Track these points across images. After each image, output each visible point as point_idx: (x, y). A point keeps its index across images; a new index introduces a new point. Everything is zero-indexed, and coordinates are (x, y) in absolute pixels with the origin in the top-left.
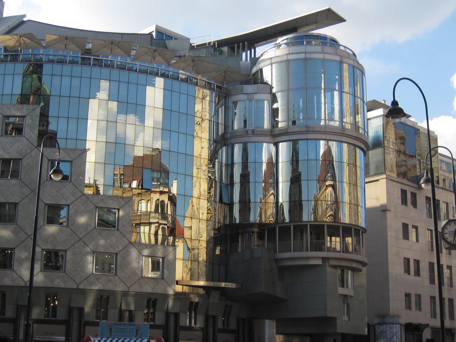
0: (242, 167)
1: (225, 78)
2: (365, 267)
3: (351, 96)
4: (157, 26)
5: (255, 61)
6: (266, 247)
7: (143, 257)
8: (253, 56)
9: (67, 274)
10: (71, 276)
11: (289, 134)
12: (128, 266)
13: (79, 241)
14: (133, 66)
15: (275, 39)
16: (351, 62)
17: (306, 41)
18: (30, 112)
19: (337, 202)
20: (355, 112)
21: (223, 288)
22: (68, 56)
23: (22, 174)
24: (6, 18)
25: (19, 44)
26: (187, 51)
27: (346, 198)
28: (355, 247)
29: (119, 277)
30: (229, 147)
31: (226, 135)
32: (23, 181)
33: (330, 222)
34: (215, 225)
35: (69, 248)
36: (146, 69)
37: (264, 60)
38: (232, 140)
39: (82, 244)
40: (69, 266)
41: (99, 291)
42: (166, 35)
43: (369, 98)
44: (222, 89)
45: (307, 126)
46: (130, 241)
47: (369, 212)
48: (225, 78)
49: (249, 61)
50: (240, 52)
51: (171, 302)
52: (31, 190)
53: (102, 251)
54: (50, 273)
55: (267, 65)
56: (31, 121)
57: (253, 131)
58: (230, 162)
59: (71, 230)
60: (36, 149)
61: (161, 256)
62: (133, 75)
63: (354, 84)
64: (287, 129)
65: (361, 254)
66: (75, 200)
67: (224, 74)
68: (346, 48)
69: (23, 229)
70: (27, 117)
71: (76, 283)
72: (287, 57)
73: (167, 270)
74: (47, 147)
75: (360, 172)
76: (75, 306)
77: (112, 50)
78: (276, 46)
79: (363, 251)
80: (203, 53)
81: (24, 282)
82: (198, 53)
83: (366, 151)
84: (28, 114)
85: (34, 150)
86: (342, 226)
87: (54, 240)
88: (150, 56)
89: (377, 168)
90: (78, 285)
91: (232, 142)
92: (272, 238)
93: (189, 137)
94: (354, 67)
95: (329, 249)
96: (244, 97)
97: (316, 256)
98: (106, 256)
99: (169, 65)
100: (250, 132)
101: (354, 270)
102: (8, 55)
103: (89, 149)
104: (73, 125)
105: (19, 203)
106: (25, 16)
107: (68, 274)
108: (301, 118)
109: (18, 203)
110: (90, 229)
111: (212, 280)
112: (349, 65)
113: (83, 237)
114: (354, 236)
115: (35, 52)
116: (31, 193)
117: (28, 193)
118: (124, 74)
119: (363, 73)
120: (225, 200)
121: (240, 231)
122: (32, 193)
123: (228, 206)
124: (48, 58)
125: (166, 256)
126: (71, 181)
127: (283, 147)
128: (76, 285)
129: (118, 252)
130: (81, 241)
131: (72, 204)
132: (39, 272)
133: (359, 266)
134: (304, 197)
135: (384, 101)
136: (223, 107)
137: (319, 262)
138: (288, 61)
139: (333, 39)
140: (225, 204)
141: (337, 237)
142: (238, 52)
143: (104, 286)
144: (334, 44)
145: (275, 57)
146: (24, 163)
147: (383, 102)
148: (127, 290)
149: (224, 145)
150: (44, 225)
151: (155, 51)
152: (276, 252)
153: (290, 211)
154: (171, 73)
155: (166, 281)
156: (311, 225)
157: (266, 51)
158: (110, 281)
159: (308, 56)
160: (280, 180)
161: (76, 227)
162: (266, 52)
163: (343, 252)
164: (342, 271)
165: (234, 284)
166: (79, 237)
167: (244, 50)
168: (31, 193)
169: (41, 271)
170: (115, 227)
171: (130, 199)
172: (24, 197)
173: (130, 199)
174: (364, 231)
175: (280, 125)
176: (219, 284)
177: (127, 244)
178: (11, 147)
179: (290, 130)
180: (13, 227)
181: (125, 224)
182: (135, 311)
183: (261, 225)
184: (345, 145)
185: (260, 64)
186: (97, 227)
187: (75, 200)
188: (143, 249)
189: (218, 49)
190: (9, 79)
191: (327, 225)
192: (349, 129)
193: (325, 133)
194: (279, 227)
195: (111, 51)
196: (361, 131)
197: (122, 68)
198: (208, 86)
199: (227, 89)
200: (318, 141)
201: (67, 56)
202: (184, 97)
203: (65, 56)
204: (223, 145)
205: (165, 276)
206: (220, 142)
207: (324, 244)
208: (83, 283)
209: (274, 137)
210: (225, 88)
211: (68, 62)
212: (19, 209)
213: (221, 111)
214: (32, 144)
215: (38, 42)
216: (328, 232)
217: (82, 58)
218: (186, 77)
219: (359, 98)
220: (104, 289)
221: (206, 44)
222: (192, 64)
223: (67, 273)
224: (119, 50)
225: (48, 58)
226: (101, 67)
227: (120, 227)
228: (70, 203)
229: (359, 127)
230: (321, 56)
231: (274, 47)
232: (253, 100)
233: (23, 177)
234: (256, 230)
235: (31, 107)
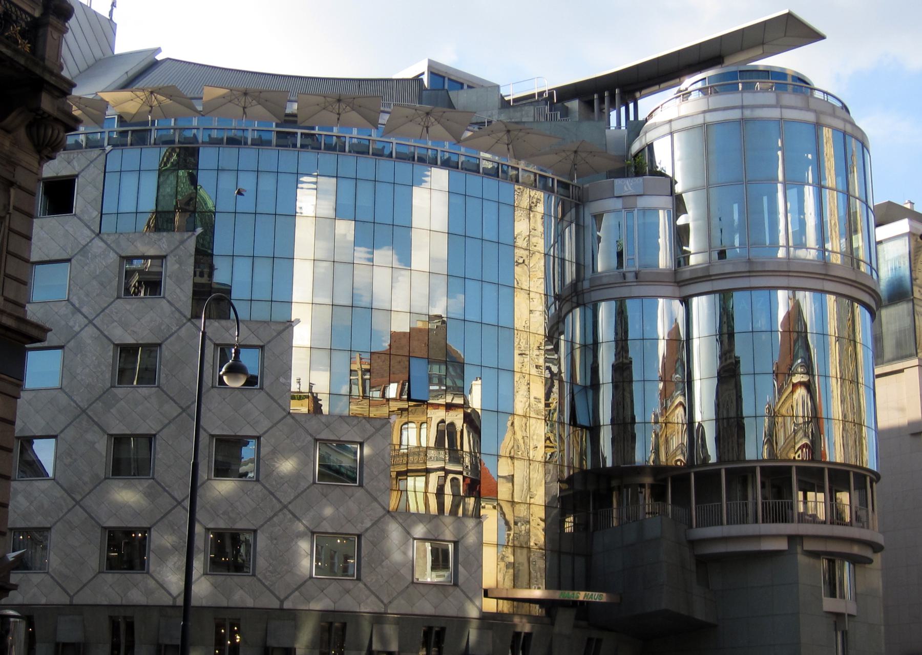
0: (616, 348)
1: (575, 165)
2: (879, 554)
3: (841, 195)
4: (430, 61)
5: (636, 127)
6: (670, 516)
7: (415, 541)
8: (632, 118)
9: (259, 580)
10: (266, 584)
11: (713, 278)
12: (383, 561)
13: (281, 510)
14: (384, 147)
15: (677, 80)
16: (839, 124)
17: (743, 83)
18: (175, 249)
19: (816, 419)
20: (850, 229)
21: (582, 602)
22: (250, 129)
23: (163, 376)
24: (121, 56)
25: (149, 108)
26: (496, 112)
27: (836, 409)
28: (856, 512)
29: (365, 585)
30: (586, 308)
31: (580, 284)
32: (165, 389)
33: (802, 460)
34: (562, 471)
35: (262, 525)
36: (411, 152)
37: (655, 126)
38: (592, 293)
39: (288, 517)
40: (261, 563)
41: (324, 613)
42: (449, 79)
43: (878, 198)
44: (569, 189)
45: (750, 261)
46: (387, 508)
47: (885, 437)
48: (575, 165)
49: (624, 128)
50: (604, 111)
51: (473, 634)
52: (181, 407)
53: (330, 531)
54: (224, 576)
55: (664, 136)
56: (177, 266)
57: (637, 275)
58: (590, 340)
60: (189, 323)
61: (452, 539)
62: (385, 165)
63: (845, 170)
64: (707, 268)
65: (871, 525)
66: (271, 428)
67: (572, 157)
68: (828, 94)
69: (167, 489)
70: (168, 258)
71: (278, 598)
72: (704, 117)
73: (464, 567)
74: (213, 319)
75: (864, 354)
76: (276, 645)
77: (339, 114)
78: (680, 96)
79: (874, 520)
80: (528, 114)
81: (170, 597)
82: (518, 114)
83: (875, 309)
84: (172, 252)
85: (184, 324)
86: (829, 469)
87: (230, 509)
88: (419, 124)
89: (899, 345)
90: (282, 602)
91: (593, 300)
92: (681, 498)
93: (503, 291)
94: (845, 133)
95: (802, 518)
96: (617, 204)
97: (774, 532)
98: (339, 541)
99: (459, 142)
100: (630, 277)
101: (857, 561)
102: (127, 132)
103: (298, 321)
104: (263, 269)
105: (157, 436)
106: (158, 50)
107: (261, 579)
108: (737, 243)
109: (155, 435)
110: (304, 485)
111: (559, 587)
112: (835, 129)
113: (290, 503)
114: (854, 490)
115: (182, 124)
117: (175, 414)
118: (366, 165)
119: (864, 145)
120: (583, 419)
121: (614, 483)
122: (184, 414)
123: (588, 432)
124: (209, 136)
125: (463, 537)
126: (261, 388)
127: (701, 306)
128: (278, 603)
129: (362, 531)
130: (285, 511)
131: (265, 436)
132: (201, 576)
133: (868, 553)
134: (747, 410)
135: (911, 203)
136: (573, 225)
137: (783, 545)
138: (706, 127)
139: (800, 77)
140: (582, 427)
141: (818, 492)
142: (601, 110)
143: (335, 603)
144: (802, 86)
145: (680, 118)
146: (166, 352)
147: (908, 206)
148: (383, 610)
149: (578, 305)
150: (208, 479)
151: (428, 114)
152: (691, 527)
153: (718, 439)
154: (462, 159)
155: (462, 591)
156: (762, 468)
157: (658, 107)
158: (348, 592)
159: (748, 113)
160: (697, 374)
162: (660, 109)
163: (831, 523)
164: (832, 563)
165: (604, 595)
166: (281, 502)
167: (612, 105)
169: (205, 574)
170: (354, 480)
171: (385, 421)
172: (167, 422)
173: (385, 421)
174: (874, 477)
175: (693, 260)
176: (574, 594)
177: (381, 514)
178: (139, 319)
179: (714, 271)
181: (376, 473)
182: (399, 652)
183: (658, 470)
184: (831, 300)
185: (647, 134)
186: (318, 481)
187: (271, 428)
188: (415, 523)
189: (559, 104)
190: (129, 181)
191: (797, 467)
192: (838, 265)
193: (787, 273)
194: (695, 473)
195: (337, 116)
196: (864, 268)
197: (361, 150)
198: (541, 183)
199: (579, 188)
200: (772, 292)
201: (247, 130)
202: (490, 208)
203: (243, 130)
204: (574, 305)
205: (461, 580)
206: (567, 299)
207: (791, 507)
208: (292, 596)
209: (680, 286)
210: (576, 187)
211: (249, 142)
212: (158, 448)
213: (569, 235)
214: (181, 313)
215: (187, 103)
216: (799, 481)
217: (278, 132)
218: (493, 167)
219: (857, 198)
220: (336, 610)
221: (533, 96)
222: (505, 137)
223: (259, 576)
224: (354, 116)
225: (209, 136)
226: (319, 151)
227: (365, 481)
228: (261, 433)
229: (858, 260)
230: (775, 113)
231: (677, 97)
232: (636, 209)
233: (163, 381)
234: (648, 480)
235: (177, 236)
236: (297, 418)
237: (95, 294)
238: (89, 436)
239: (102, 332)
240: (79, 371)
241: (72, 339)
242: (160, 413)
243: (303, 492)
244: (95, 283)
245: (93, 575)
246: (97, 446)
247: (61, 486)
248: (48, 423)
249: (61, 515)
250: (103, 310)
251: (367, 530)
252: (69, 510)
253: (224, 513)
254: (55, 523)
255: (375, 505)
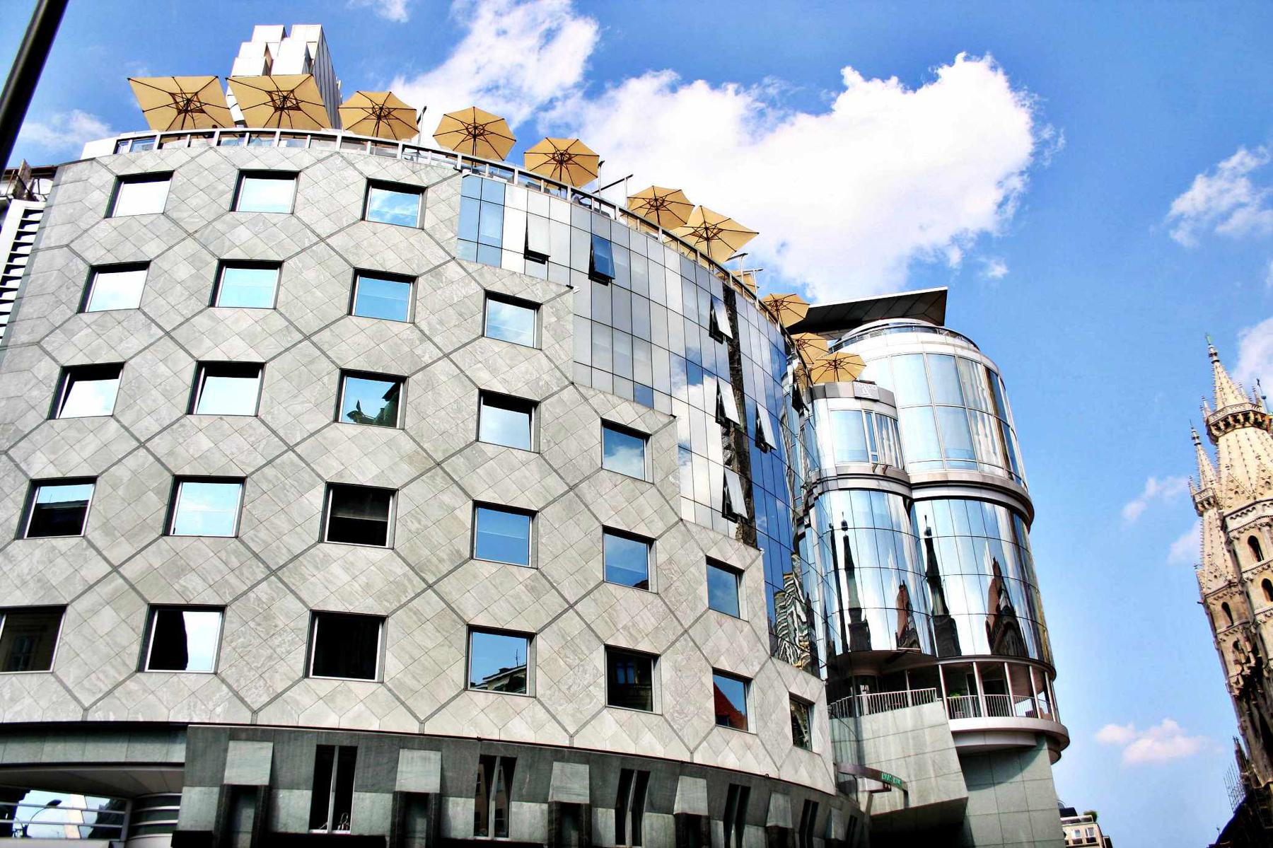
9: (666, 720)
13: (683, 634)
56: (554, 319)
59: (665, 603)
69: (555, 584)
87: (631, 624)
100: (879, 471)
116: (567, 492)
122: (571, 493)
161: (673, 599)
168: (567, 492)
180: (529, 575)
236: (688, 525)
237: (452, 324)
238: (446, 498)
239: (462, 371)
240: (429, 412)
241: (419, 371)
242: (543, 486)
243: (701, 616)
244: (451, 310)
245: (456, 693)
246: (457, 512)
247: (404, 560)
248: (383, 471)
249: (404, 600)
250: (464, 345)
251: (758, 673)
252: (418, 595)
253: (625, 627)
254: (394, 611)
255: (759, 645)
